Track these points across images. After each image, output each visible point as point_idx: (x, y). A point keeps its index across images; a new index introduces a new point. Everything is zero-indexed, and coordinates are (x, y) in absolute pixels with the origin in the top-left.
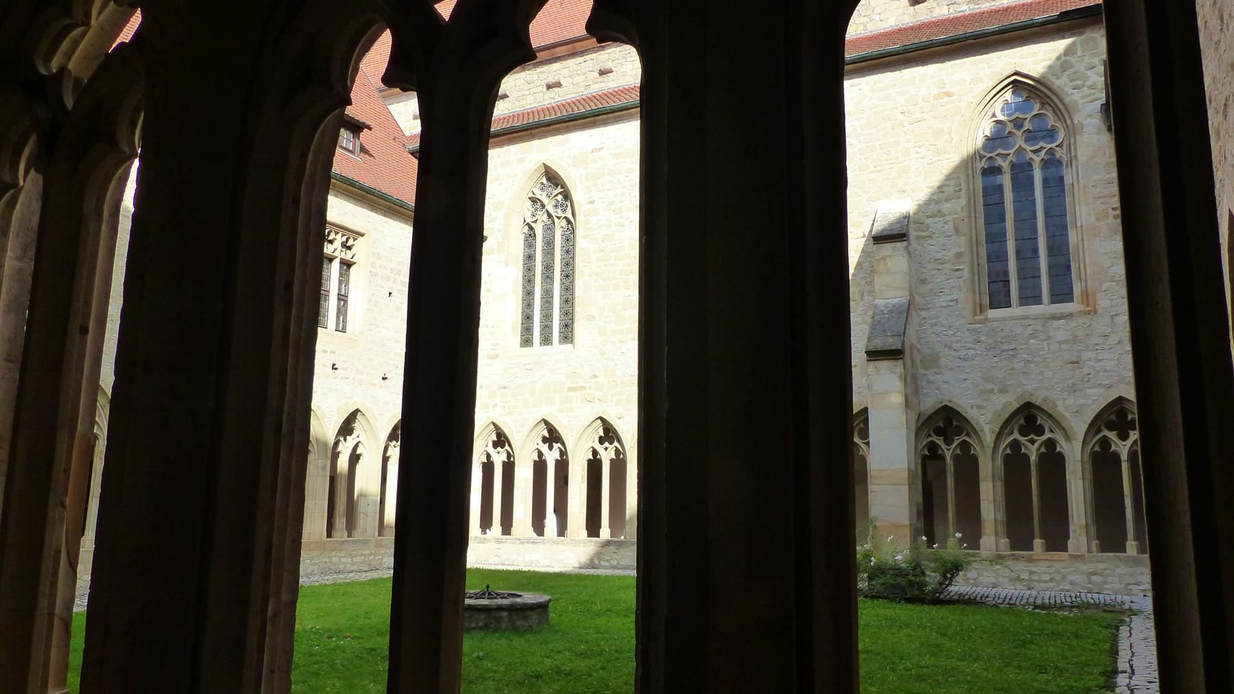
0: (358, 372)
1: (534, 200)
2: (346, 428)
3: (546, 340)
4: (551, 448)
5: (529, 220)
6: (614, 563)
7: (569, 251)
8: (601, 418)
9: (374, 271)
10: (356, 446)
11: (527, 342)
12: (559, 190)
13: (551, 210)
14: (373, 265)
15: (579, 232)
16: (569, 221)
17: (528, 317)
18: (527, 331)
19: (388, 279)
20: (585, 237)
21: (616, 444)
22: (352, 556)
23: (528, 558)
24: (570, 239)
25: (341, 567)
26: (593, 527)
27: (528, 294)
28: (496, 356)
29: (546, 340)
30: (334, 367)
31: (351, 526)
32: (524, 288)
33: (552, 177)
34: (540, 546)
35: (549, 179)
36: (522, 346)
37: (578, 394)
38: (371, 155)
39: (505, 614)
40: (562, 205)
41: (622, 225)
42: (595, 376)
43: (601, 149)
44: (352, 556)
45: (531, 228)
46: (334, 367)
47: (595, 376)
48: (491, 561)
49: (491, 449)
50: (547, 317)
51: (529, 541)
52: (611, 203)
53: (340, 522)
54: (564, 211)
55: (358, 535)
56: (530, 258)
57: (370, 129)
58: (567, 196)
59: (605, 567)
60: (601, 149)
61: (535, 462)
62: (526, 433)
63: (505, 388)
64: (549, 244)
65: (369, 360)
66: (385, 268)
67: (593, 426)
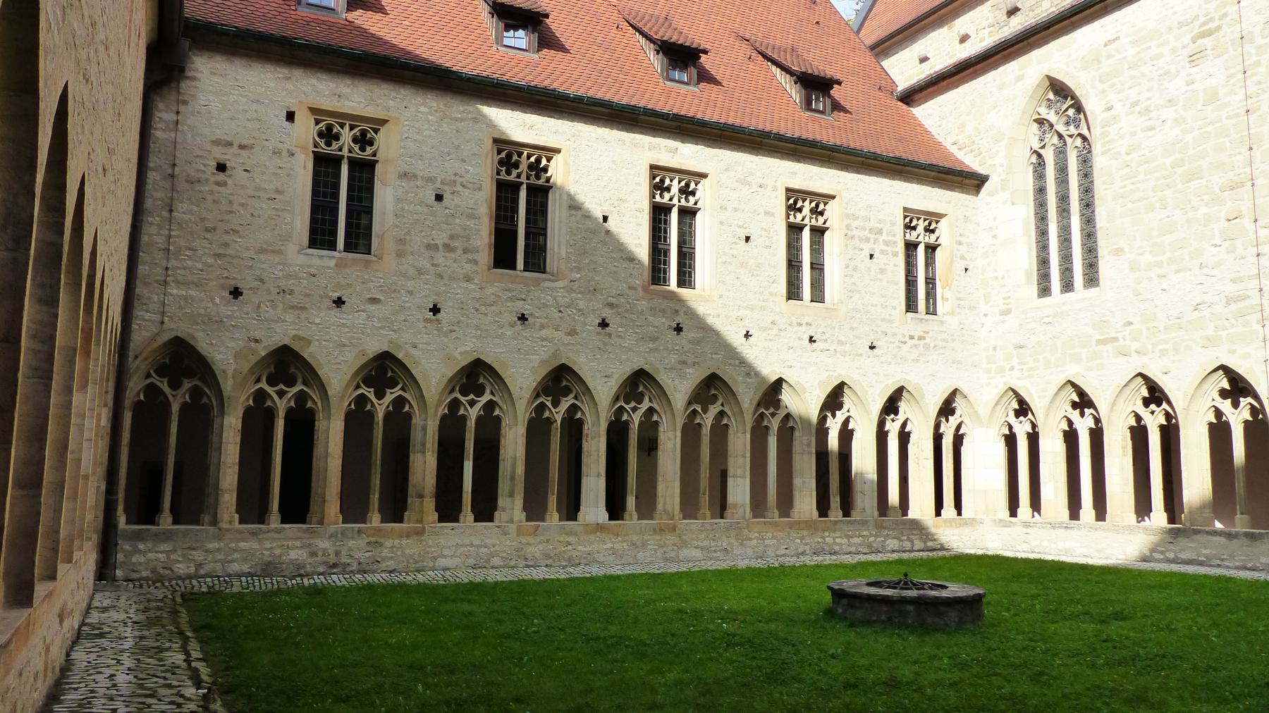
0: (840, 343)
1: (1040, 122)
2: (834, 400)
3: (1068, 286)
4: (1082, 414)
5: (1036, 146)
6: (1172, 555)
7: (1086, 175)
8: (1140, 374)
9: (849, 233)
10: (847, 421)
11: (1045, 291)
12: (1069, 102)
13: (1060, 128)
14: (848, 227)
15: (1097, 149)
16: (1084, 139)
17: (1044, 262)
18: (1044, 277)
19: (868, 240)
20: (1103, 153)
21: (1165, 405)
22: (849, 537)
23: (1061, 545)
24: (1086, 161)
25: (837, 548)
26: (1143, 507)
27: (1043, 234)
28: (1008, 312)
29: (1068, 286)
30: (811, 340)
31: (847, 509)
32: (1037, 227)
33: (1059, 90)
34: (1075, 532)
35: (1056, 93)
36: (1040, 296)
37: (1109, 347)
38: (847, 111)
39: (911, 608)
40: (1075, 120)
41: (1152, 128)
42: (1130, 323)
43: (1118, 38)
44: (849, 537)
45: (1040, 156)
46: (811, 340)
47: (1130, 323)
48: (1019, 548)
49: (1012, 419)
50: (1066, 258)
51: (1060, 526)
52: (1134, 104)
53: (835, 501)
54: (1077, 127)
55: (856, 515)
56: (1041, 191)
57: (839, 83)
58: (1079, 108)
59: (1158, 561)
60: (1118, 38)
61: (1131, 428)
62: (1049, 398)
63: (1021, 347)
64: (1062, 170)
65: (852, 329)
66: (864, 229)
67: (1133, 385)
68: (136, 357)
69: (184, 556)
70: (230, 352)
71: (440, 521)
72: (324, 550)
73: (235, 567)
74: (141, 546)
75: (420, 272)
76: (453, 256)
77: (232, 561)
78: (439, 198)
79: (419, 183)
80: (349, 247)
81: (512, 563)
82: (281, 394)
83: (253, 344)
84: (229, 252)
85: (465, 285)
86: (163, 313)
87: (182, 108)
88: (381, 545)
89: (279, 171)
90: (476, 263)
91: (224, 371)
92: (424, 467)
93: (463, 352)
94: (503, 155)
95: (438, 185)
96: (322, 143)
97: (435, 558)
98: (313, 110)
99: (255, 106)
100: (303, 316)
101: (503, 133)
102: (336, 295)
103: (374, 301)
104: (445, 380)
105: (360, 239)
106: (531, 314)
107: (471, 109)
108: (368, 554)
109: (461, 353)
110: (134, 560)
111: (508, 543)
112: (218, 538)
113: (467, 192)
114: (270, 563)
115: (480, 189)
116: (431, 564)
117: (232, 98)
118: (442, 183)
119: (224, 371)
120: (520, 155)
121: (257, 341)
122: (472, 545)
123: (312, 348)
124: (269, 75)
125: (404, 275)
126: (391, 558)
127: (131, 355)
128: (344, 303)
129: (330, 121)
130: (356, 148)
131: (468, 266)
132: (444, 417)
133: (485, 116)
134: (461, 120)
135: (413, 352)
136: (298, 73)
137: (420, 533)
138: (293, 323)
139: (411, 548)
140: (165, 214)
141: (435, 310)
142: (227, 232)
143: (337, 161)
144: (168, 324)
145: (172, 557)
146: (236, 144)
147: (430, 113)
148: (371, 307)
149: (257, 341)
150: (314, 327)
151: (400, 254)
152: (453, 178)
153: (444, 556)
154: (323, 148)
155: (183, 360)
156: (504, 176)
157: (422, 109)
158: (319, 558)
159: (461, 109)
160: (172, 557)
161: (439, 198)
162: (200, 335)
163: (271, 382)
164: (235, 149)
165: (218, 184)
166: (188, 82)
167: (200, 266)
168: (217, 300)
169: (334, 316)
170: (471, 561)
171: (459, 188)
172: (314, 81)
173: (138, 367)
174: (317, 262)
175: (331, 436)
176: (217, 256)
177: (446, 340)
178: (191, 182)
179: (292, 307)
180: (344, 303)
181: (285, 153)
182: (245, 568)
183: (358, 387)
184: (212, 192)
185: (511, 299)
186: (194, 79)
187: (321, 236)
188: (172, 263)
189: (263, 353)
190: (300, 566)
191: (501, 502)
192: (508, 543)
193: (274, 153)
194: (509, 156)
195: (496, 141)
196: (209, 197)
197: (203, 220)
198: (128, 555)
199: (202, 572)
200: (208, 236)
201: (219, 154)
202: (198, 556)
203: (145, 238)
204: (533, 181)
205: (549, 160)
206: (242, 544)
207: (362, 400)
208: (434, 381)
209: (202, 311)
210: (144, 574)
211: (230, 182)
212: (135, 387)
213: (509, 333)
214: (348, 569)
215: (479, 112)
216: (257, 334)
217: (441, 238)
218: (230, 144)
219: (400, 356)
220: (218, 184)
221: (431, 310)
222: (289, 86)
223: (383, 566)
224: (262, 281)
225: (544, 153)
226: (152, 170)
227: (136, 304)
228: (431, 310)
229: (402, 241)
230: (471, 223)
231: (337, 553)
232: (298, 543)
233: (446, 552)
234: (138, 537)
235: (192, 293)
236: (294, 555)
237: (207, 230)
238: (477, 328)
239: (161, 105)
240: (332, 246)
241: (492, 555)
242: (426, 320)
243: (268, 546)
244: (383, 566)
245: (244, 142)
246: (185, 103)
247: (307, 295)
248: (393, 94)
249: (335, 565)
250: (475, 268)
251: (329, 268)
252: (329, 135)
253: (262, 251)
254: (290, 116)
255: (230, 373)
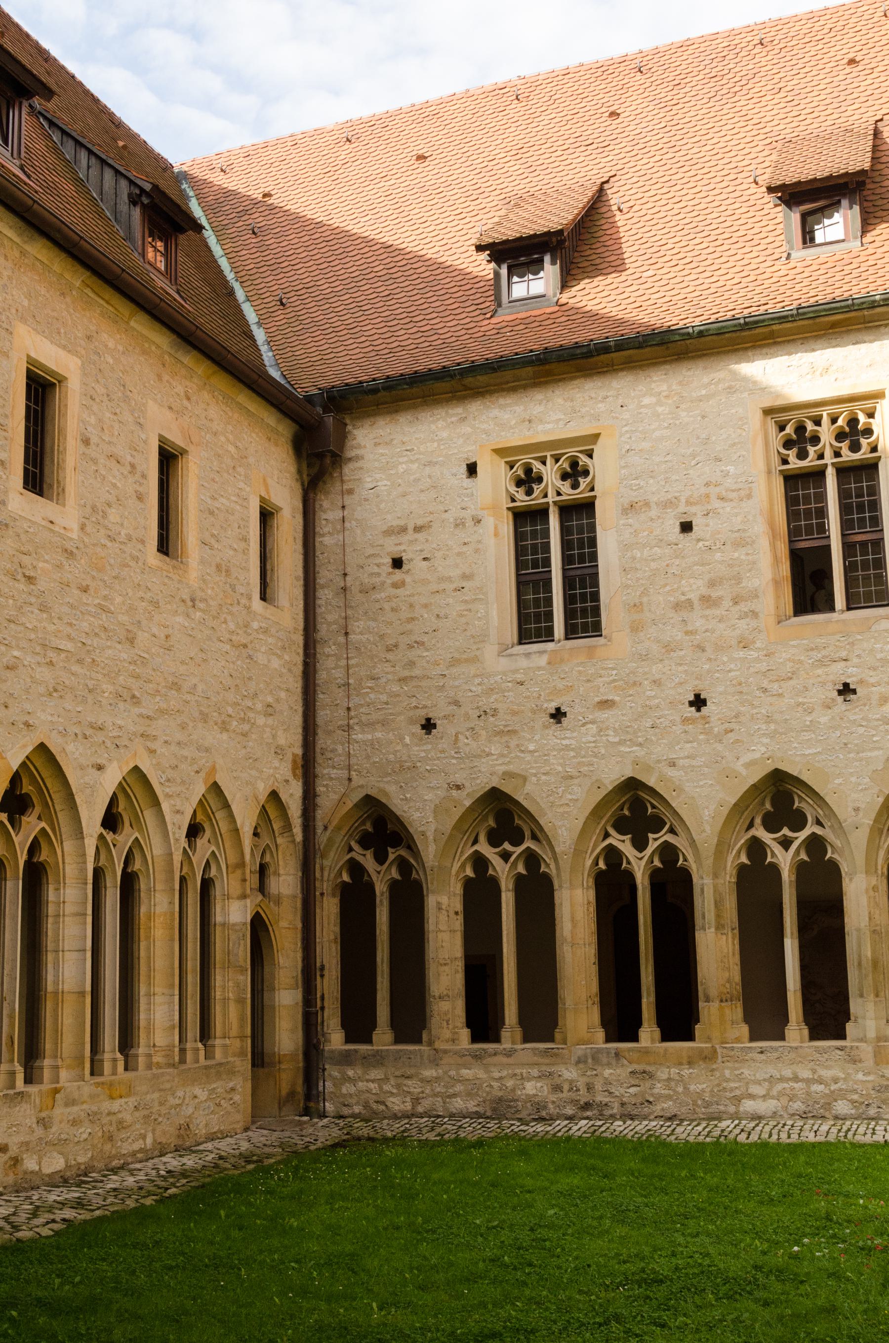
68: (326, 828)
69: (398, 1086)
70: (428, 810)
71: (752, 1039)
72: (571, 1082)
73: (458, 1104)
74: (350, 1073)
75: (668, 648)
76: (717, 612)
77: (455, 1095)
78: (686, 527)
79: (653, 513)
80: (571, 632)
81: (872, 1112)
82: (505, 856)
83: (454, 793)
84: (417, 672)
85: (741, 654)
86: (349, 768)
87: (348, 500)
88: (651, 1076)
89: (465, 549)
90: (755, 614)
91: (423, 834)
92: (717, 952)
93: (750, 763)
94: (789, 429)
95: (682, 508)
96: (520, 495)
97: (738, 1100)
98: (500, 452)
99: (428, 470)
100: (513, 743)
101: (778, 396)
102: (551, 707)
103: (606, 704)
104: (725, 811)
105: (585, 619)
106: (861, 682)
107: (721, 375)
108: (632, 1090)
109: (747, 765)
110: (344, 1091)
111: (860, 1076)
112: (435, 1062)
113: (728, 508)
114: (500, 1099)
115: (749, 496)
116: (732, 1109)
117: (401, 469)
118: (688, 503)
119: (423, 834)
120: (818, 423)
121: (458, 787)
122: (796, 1079)
123: (528, 788)
124: (441, 424)
125: (644, 657)
126: (669, 1097)
127: (320, 825)
128: (565, 714)
129: (525, 458)
130: (565, 487)
131: (742, 624)
132: (742, 870)
133: (745, 379)
134: (708, 397)
135: (671, 772)
136: (475, 407)
137: (709, 1057)
138: (502, 755)
139: (699, 1082)
140: (341, 639)
141: (698, 702)
142: (411, 647)
143: (541, 513)
144: (357, 780)
145: (386, 1087)
146: (411, 527)
147: (659, 403)
148: (603, 715)
149: (458, 787)
150: (528, 757)
151: (635, 628)
152: (703, 490)
153: (751, 1097)
154: (522, 499)
155: (381, 828)
156: (795, 464)
157: (646, 401)
158: (565, 1095)
159: (706, 380)
160: (386, 1087)
161: (686, 527)
162: (392, 789)
163: (494, 840)
164: (410, 535)
165: (395, 586)
166: (351, 465)
167: (384, 698)
168: (407, 740)
169: (554, 736)
170: (798, 1106)
171: (717, 504)
172: (495, 412)
173: (330, 840)
174: (523, 663)
175: (575, 911)
176: (403, 680)
177: (719, 747)
178: (365, 591)
179: (501, 733)
180: (564, 714)
181: (469, 523)
182: (472, 1106)
183: (607, 835)
184: (389, 599)
185: (821, 663)
186: (358, 458)
187: (532, 626)
188: (355, 701)
189: (468, 803)
190: (540, 1106)
191: (854, 1006)
192: (860, 1076)
193: (457, 525)
194: (800, 429)
195: (768, 412)
196: (387, 606)
197: (382, 637)
198: (337, 1084)
199: (420, 1109)
200: (390, 656)
201: (392, 547)
202: (414, 1087)
203: (322, 676)
204: (848, 456)
205: (871, 415)
206: (465, 1072)
207: (612, 855)
208: (706, 814)
209: (391, 757)
210: (357, 1109)
211: (408, 579)
212: (331, 869)
213: (823, 720)
214: (607, 1113)
215: (734, 373)
216: (459, 778)
217: (694, 588)
218: (403, 530)
219: (651, 782)
220: (395, 586)
221: (691, 704)
222: (466, 429)
223: (658, 1109)
224: (457, 703)
225: (856, 406)
226: (323, 587)
227: (319, 759)
228: (691, 704)
229: (637, 607)
230: (739, 554)
231: (590, 1088)
232: (535, 1072)
233: (755, 1090)
234: (346, 1059)
235: (379, 735)
236: (530, 1088)
237: (389, 650)
238: (769, 719)
239: (326, 504)
240: (547, 635)
241: (834, 1096)
242: (685, 720)
243: (496, 1075)
244: (658, 1109)
245: (420, 523)
246: (350, 492)
247: (514, 713)
248: (602, 393)
249: (587, 1106)
250: (754, 623)
251: (539, 668)
252: (528, 480)
253: (454, 662)
254: (472, 470)
255: (430, 835)
